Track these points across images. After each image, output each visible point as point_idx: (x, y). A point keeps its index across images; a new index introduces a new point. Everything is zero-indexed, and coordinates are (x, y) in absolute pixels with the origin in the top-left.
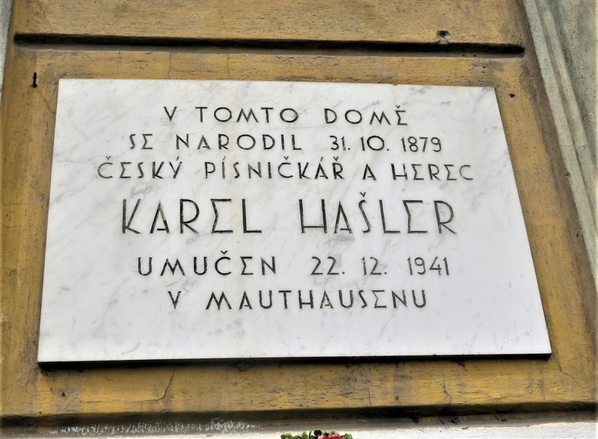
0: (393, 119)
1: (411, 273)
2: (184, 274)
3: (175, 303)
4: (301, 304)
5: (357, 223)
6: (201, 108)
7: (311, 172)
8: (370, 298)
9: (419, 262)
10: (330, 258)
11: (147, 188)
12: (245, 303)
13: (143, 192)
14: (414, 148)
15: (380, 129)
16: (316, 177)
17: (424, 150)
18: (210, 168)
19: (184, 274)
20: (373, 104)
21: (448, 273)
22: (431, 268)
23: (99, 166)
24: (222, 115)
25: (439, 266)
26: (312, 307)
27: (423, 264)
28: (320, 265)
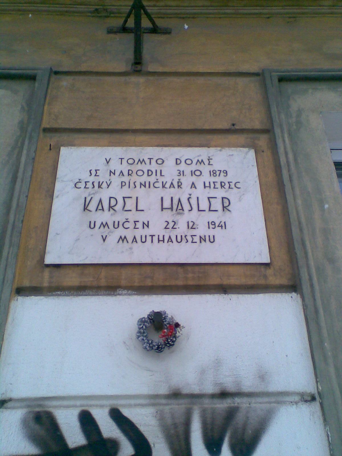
0: (206, 162)
1: (209, 228)
2: (109, 228)
3: (104, 240)
4: (159, 241)
5: (186, 207)
6: (122, 159)
7: (168, 185)
8: (189, 239)
9: (213, 223)
10: (173, 221)
11: (96, 192)
12: (135, 240)
13: (94, 194)
14: (215, 175)
15: (201, 167)
16: (170, 187)
17: (219, 176)
18: (124, 184)
19: (109, 228)
20: (198, 156)
21: (225, 228)
22: (218, 226)
23: (75, 183)
24: (131, 161)
25: (222, 225)
26: (164, 242)
27: (215, 224)
28: (169, 225)
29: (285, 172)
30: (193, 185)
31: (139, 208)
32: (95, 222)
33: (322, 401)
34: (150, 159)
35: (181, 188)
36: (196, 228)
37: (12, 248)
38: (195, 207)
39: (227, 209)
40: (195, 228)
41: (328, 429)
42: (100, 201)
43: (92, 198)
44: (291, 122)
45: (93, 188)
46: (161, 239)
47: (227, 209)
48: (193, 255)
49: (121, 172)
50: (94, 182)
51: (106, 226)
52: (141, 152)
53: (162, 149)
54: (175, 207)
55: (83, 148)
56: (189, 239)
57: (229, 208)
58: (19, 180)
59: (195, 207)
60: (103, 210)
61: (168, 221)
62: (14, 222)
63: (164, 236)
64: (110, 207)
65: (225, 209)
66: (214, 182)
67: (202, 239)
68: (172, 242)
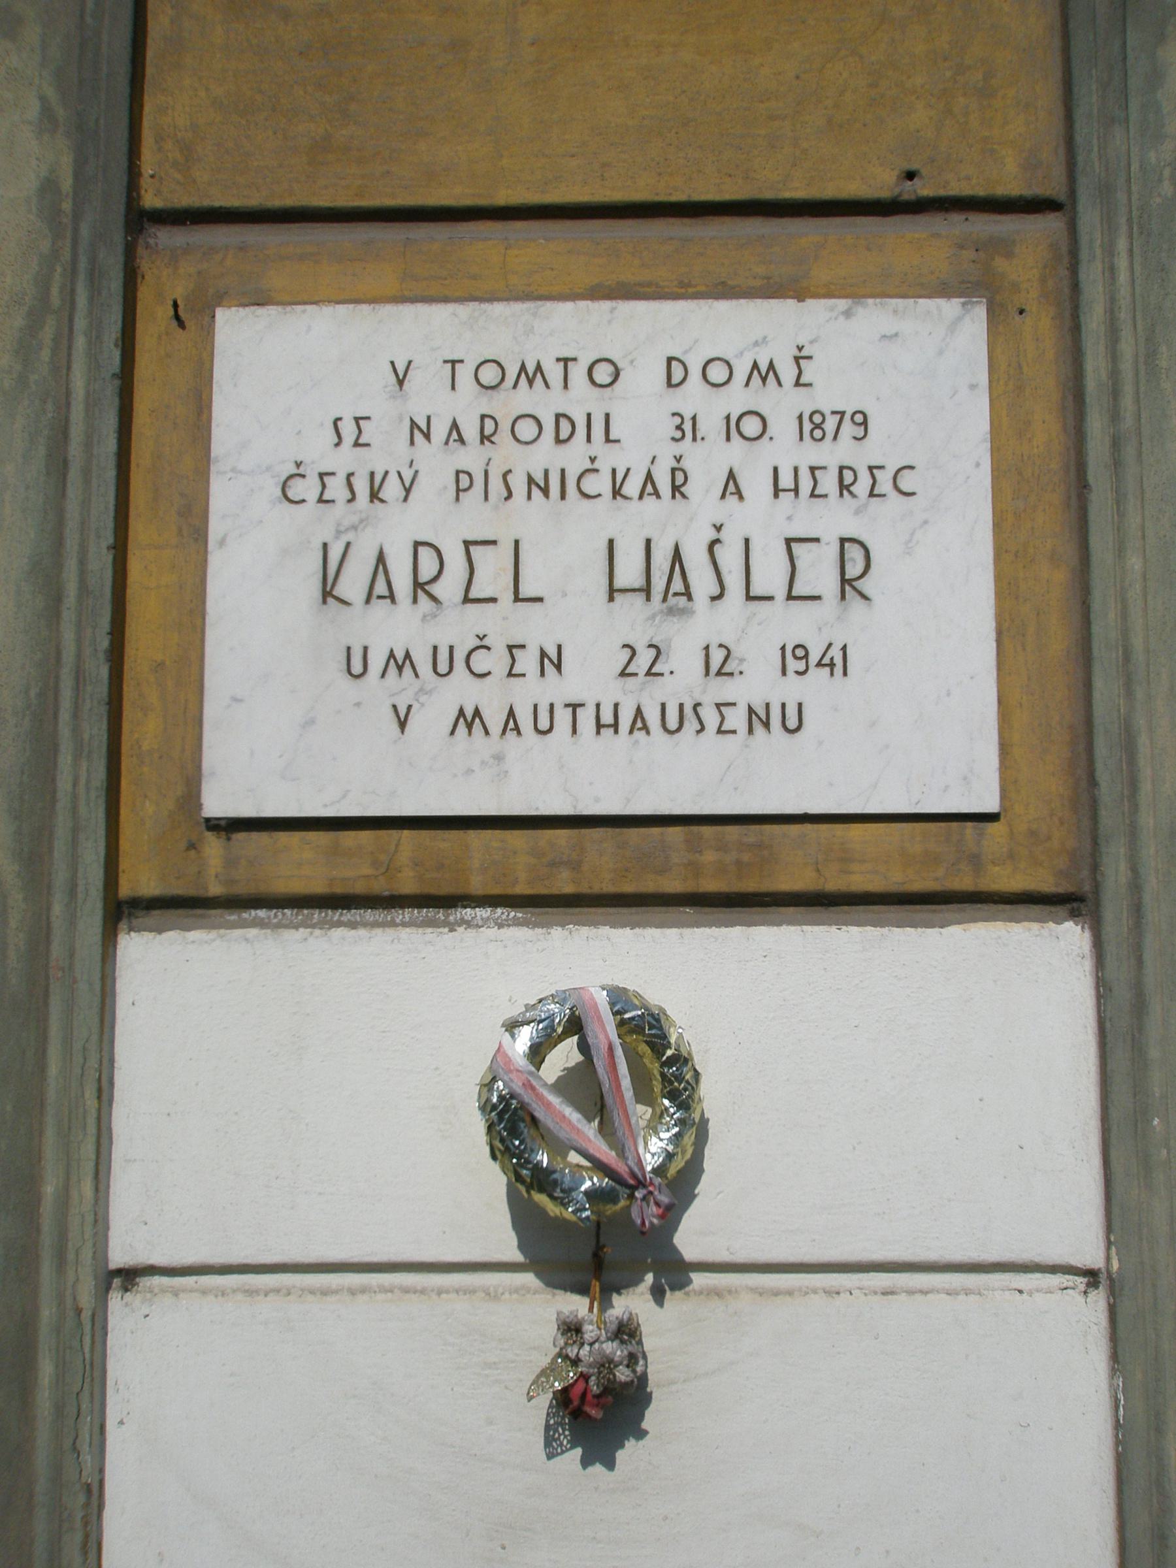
0: (787, 372)
1: (784, 673)
2: (417, 675)
3: (402, 725)
4: (599, 726)
5: (702, 581)
6: (453, 362)
7: (632, 487)
8: (711, 718)
9: (800, 652)
10: (650, 646)
11: (361, 521)
12: (511, 724)
13: (354, 528)
14: (818, 434)
15: (767, 399)
16: (641, 497)
17: (835, 438)
18: (464, 481)
19: (417, 675)
20: (756, 344)
21: (845, 674)
22: (819, 664)
23: (283, 478)
24: (489, 375)
25: (832, 659)
26: (616, 732)
27: (806, 656)
28: (635, 658)
29: (1096, 424)
30: (732, 485)
31: (525, 592)
32: (366, 649)
33: (1114, 1302)
34: (566, 361)
35: (684, 496)
36: (736, 673)
37: (84, 765)
38: (734, 581)
39: (854, 588)
40: (731, 674)
41: (1121, 1385)
42: (381, 559)
43: (348, 545)
44: (1153, 160)
45: (349, 501)
46: (606, 717)
47: (854, 588)
48: (722, 780)
49: (455, 426)
50: (352, 474)
51: (407, 669)
52: (529, 331)
53: (613, 310)
54: (658, 584)
55: (304, 311)
56: (711, 718)
57: (865, 585)
58: (74, 474)
59: (734, 581)
60: (392, 597)
61: (633, 646)
62: (79, 656)
63: (616, 706)
64: (418, 586)
65: (847, 588)
66: (813, 469)
67: (758, 719)
68: (648, 733)
